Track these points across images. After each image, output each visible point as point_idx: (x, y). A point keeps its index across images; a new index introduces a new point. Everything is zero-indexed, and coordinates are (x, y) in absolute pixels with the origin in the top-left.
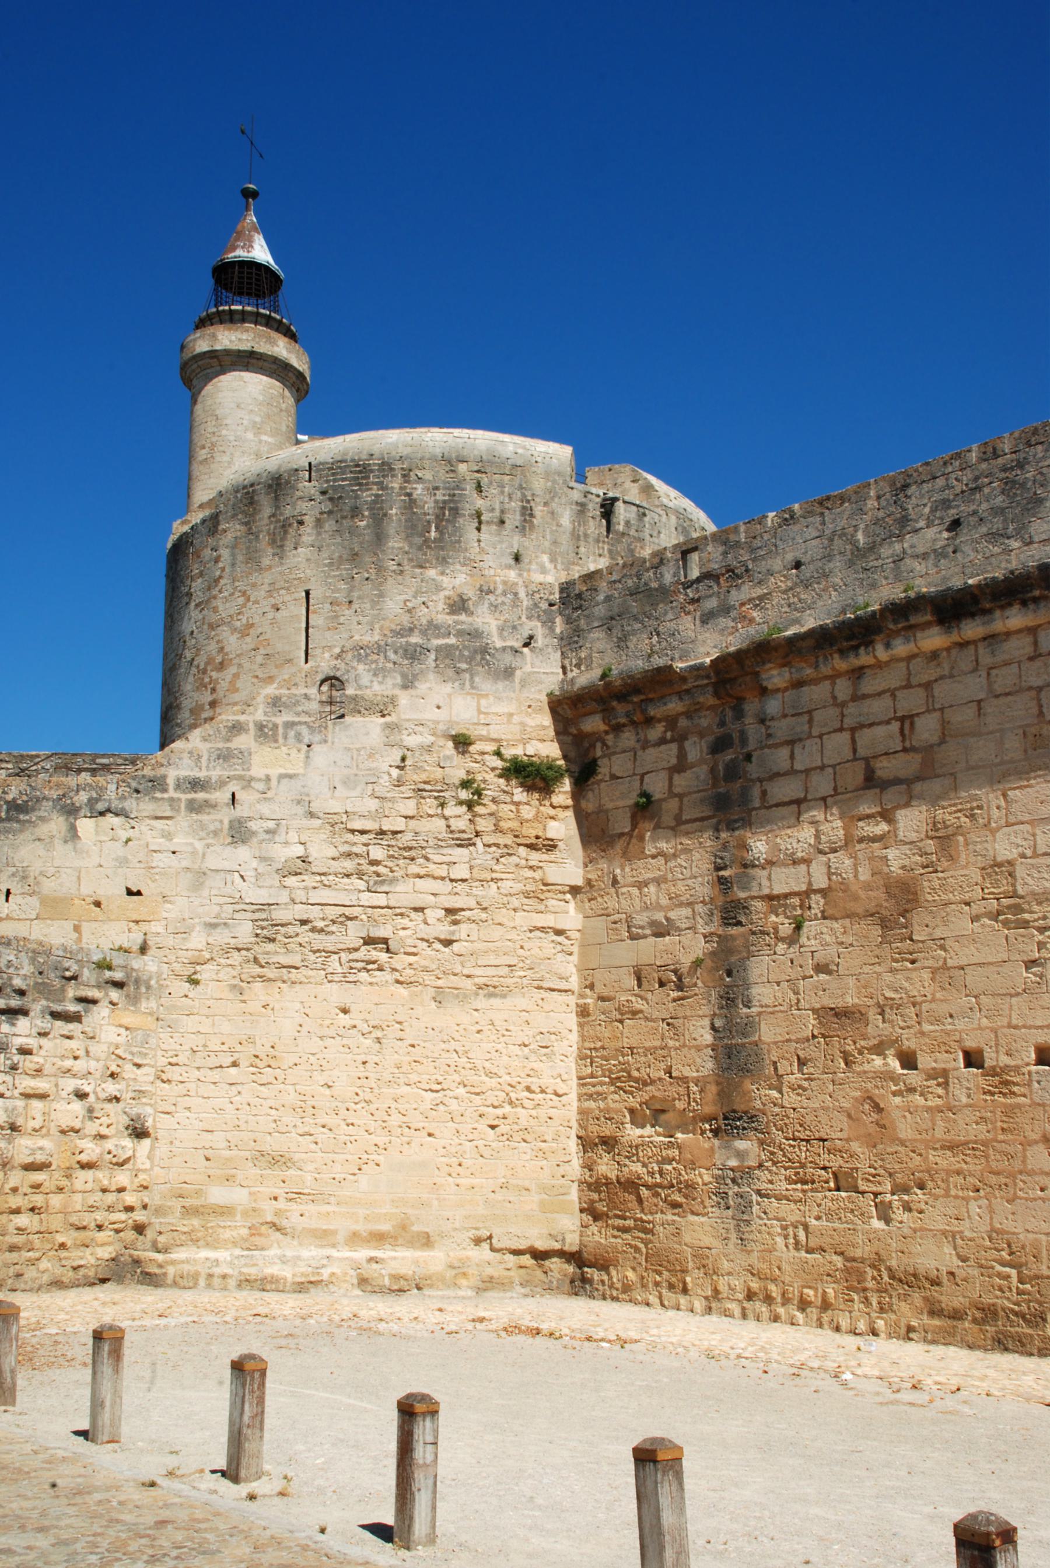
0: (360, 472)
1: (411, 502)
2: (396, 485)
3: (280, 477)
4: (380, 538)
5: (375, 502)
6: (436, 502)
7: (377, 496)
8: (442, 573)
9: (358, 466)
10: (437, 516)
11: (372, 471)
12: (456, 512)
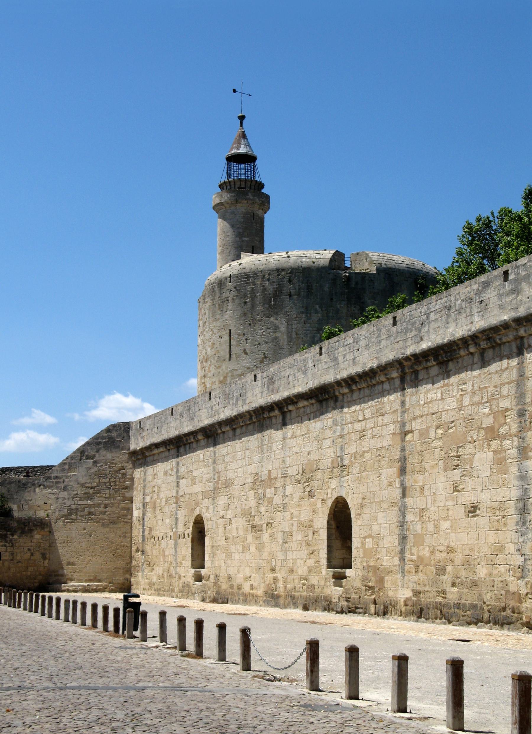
0: (246, 278)
1: (265, 289)
2: (259, 283)
3: (221, 281)
4: (253, 307)
5: (252, 290)
6: (274, 288)
7: (253, 288)
8: (276, 319)
9: (246, 275)
10: (274, 294)
11: (250, 277)
12: (281, 291)
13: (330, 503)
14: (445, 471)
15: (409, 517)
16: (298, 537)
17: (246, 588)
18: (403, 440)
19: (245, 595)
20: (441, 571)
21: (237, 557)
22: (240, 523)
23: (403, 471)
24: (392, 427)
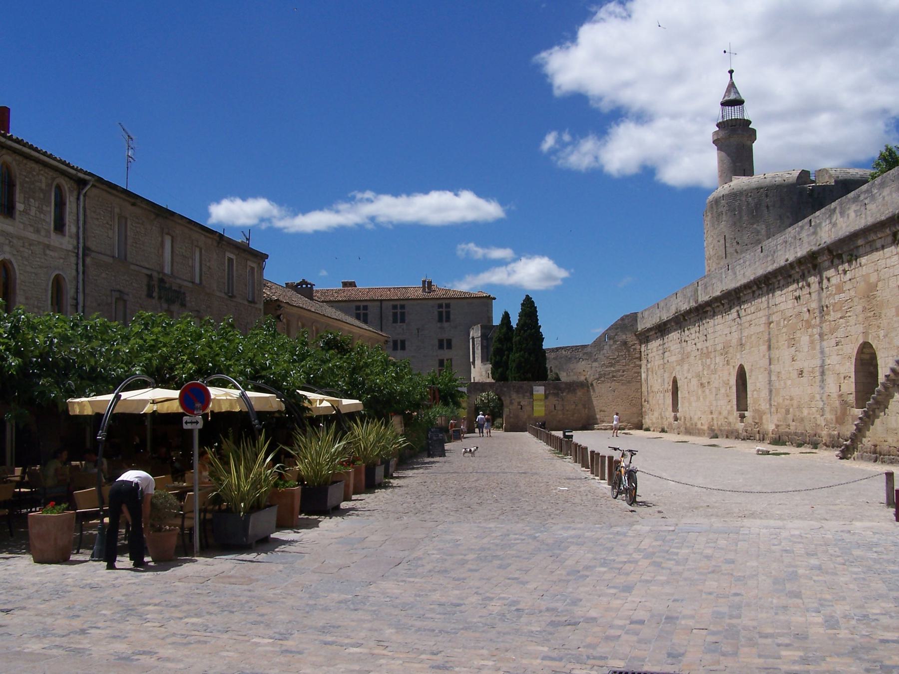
13: (737, 368)
14: (788, 347)
15: (773, 378)
16: (723, 391)
17: (699, 426)
18: (769, 327)
19: (698, 430)
20: (787, 412)
21: (694, 404)
22: (695, 382)
23: (769, 348)
24: (764, 318)
